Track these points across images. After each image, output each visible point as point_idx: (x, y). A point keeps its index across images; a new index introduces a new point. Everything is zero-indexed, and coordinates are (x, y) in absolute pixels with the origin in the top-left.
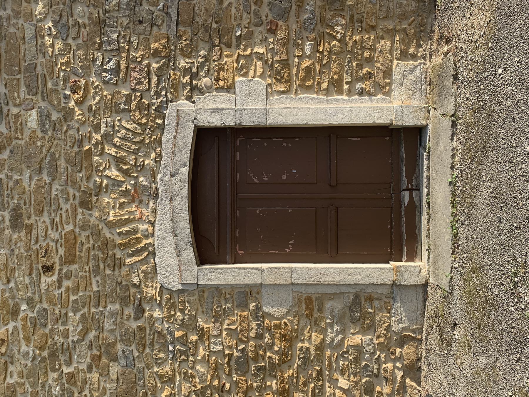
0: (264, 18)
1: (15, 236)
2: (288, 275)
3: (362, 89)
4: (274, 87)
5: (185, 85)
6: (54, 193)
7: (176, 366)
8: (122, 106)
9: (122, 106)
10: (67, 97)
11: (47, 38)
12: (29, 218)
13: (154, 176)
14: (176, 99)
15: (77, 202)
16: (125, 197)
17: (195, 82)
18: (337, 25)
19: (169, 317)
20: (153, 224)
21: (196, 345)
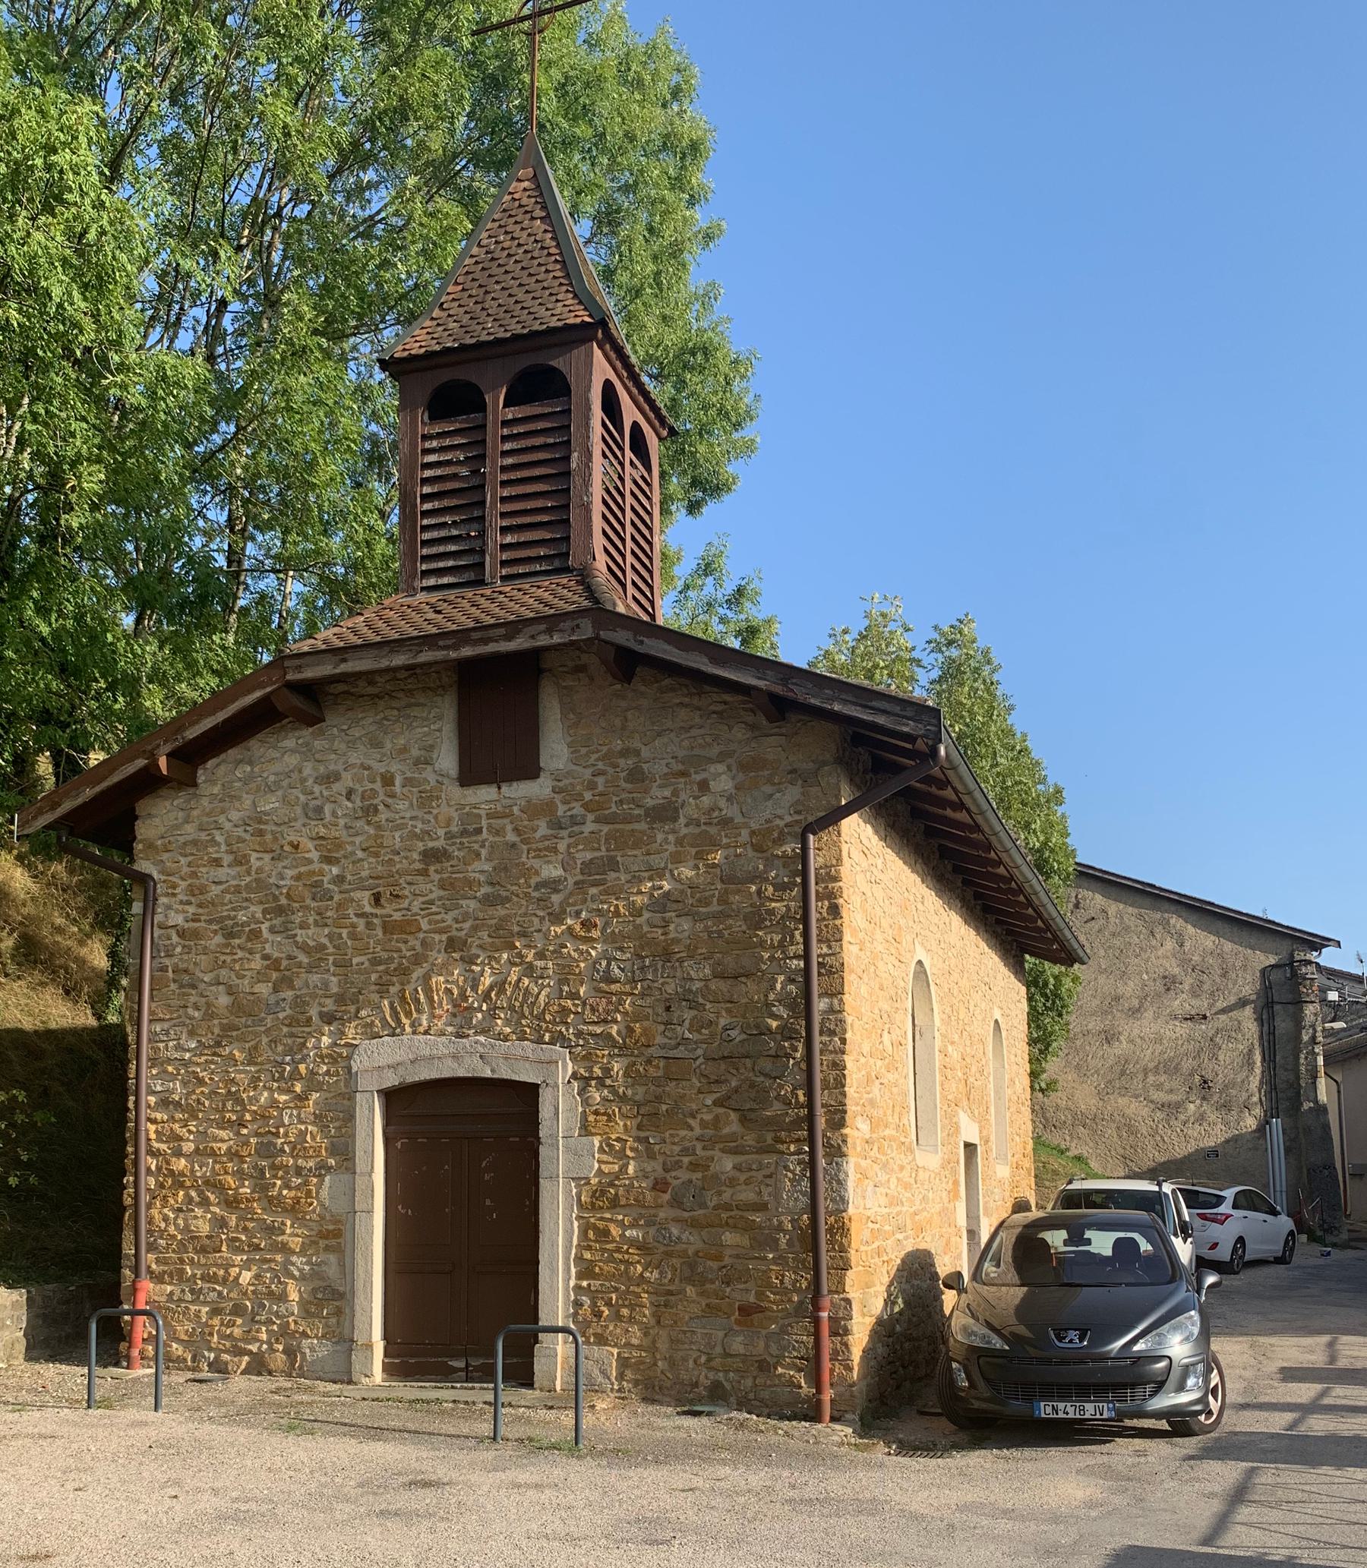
0: (673, 1174)
1: (416, 856)
2: (364, 1207)
3: (582, 1305)
4: (587, 1188)
5: (590, 1069)
6: (463, 903)
7: (267, 1067)
8: (566, 988)
9: (566, 988)
10: (578, 914)
11: (649, 885)
12: (436, 871)
13: (484, 1032)
14: (573, 1059)
15: (454, 933)
16: (459, 994)
17: (593, 1083)
18: (661, 1273)
19: (321, 1057)
20: (426, 1033)
21: (289, 1091)
